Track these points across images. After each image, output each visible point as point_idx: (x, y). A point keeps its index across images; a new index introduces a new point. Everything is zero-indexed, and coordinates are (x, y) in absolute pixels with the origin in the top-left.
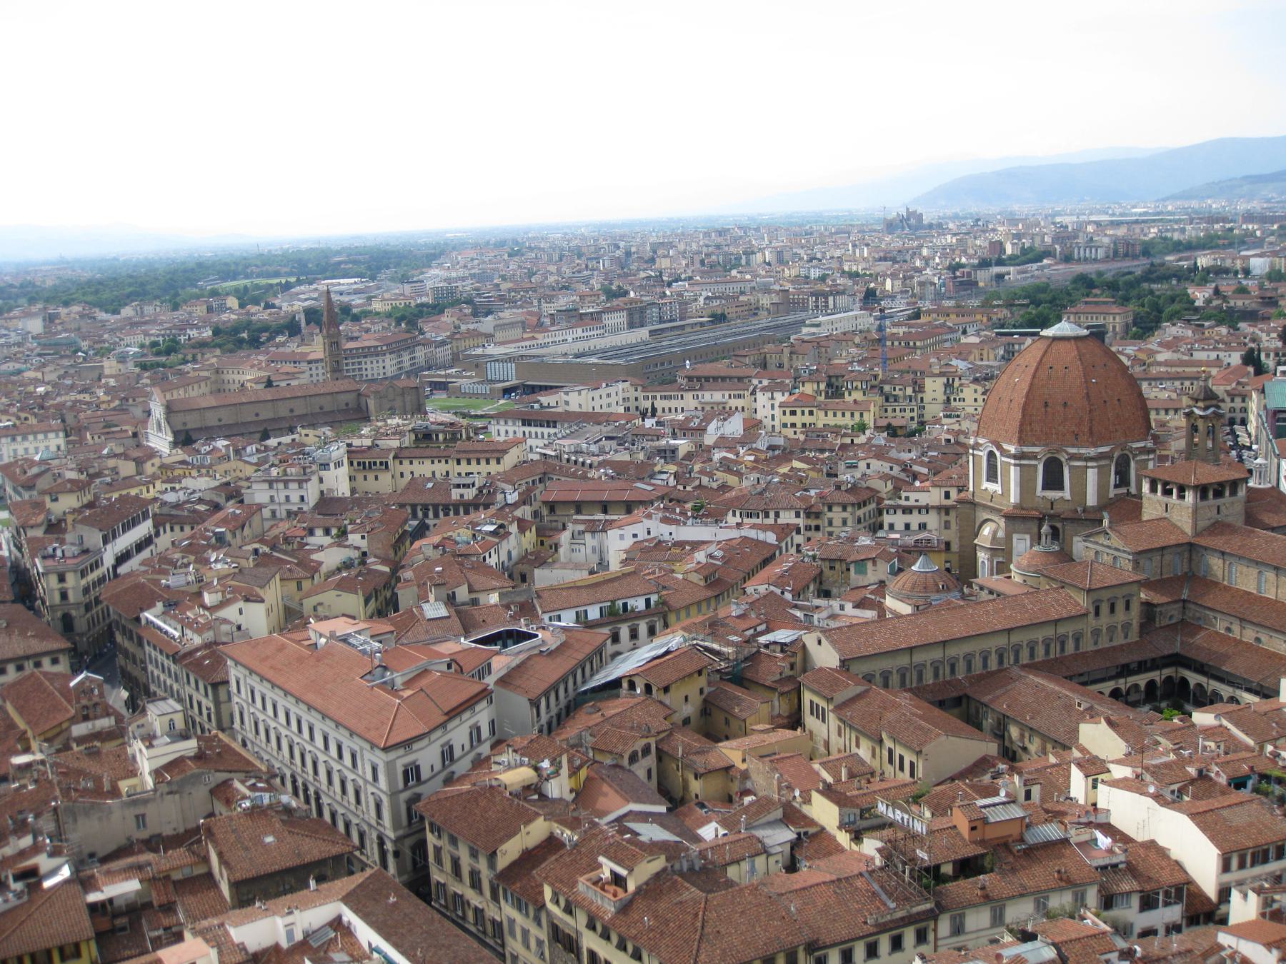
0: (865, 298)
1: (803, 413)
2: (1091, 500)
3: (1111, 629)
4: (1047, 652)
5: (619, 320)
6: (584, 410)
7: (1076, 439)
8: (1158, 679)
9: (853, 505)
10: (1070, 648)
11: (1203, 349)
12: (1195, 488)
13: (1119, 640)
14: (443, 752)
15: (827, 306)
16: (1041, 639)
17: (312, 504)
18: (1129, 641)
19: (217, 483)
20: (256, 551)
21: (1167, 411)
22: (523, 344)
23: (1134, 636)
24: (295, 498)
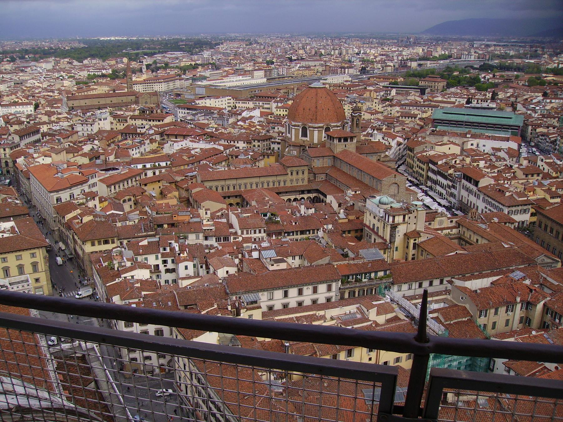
0: (361, 70)
1: (283, 111)
2: (316, 141)
3: (297, 180)
4: (274, 185)
5: (261, 74)
6: (212, 106)
7: (311, 121)
8: (311, 197)
9: (262, 140)
10: (282, 184)
11: (455, 97)
12: (336, 138)
13: (300, 183)
14: (70, 196)
15: (345, 73)
16: (271, 181)
17: (95, 132)
18: (304, 184)
19: (70, 124)
20: (69, 145)
21: (405, 117)
22: (218, 81)
23: (306, 183)
24: (90, 130)
